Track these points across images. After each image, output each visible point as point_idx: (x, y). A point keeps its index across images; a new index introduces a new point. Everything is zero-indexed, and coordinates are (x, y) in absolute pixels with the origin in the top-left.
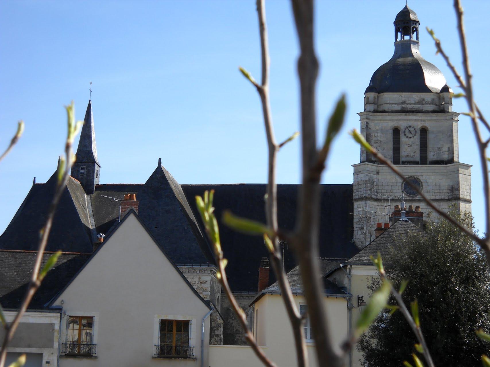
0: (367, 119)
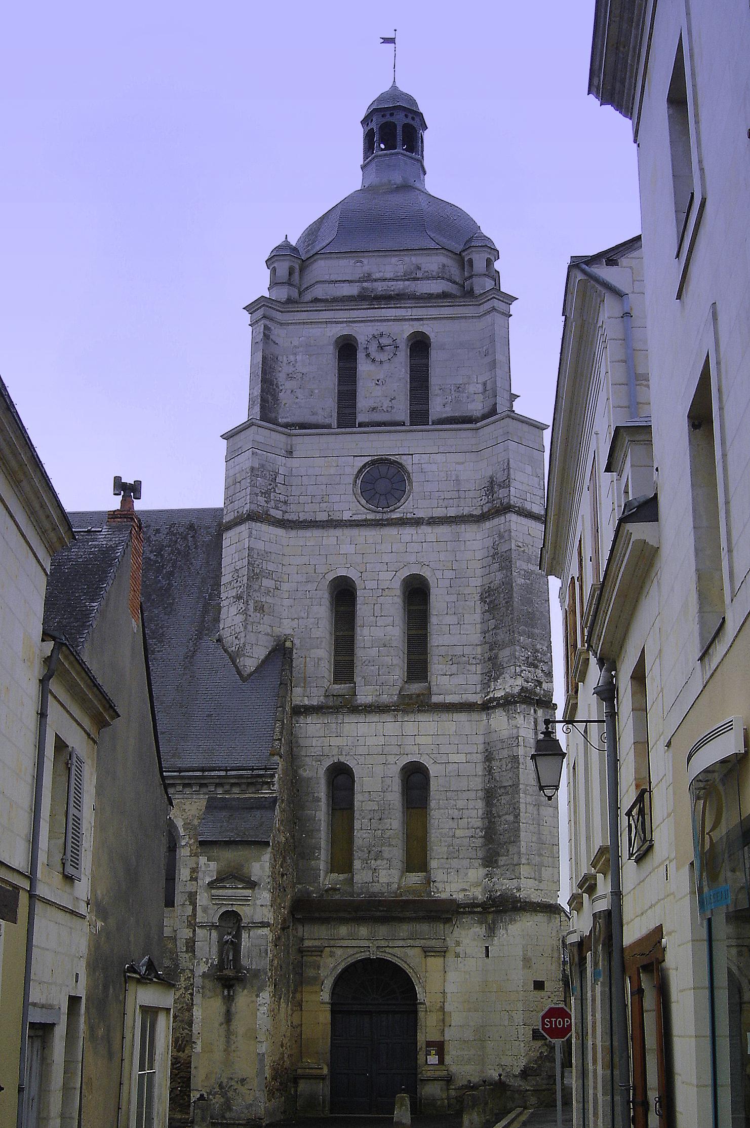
0: (264, 317)
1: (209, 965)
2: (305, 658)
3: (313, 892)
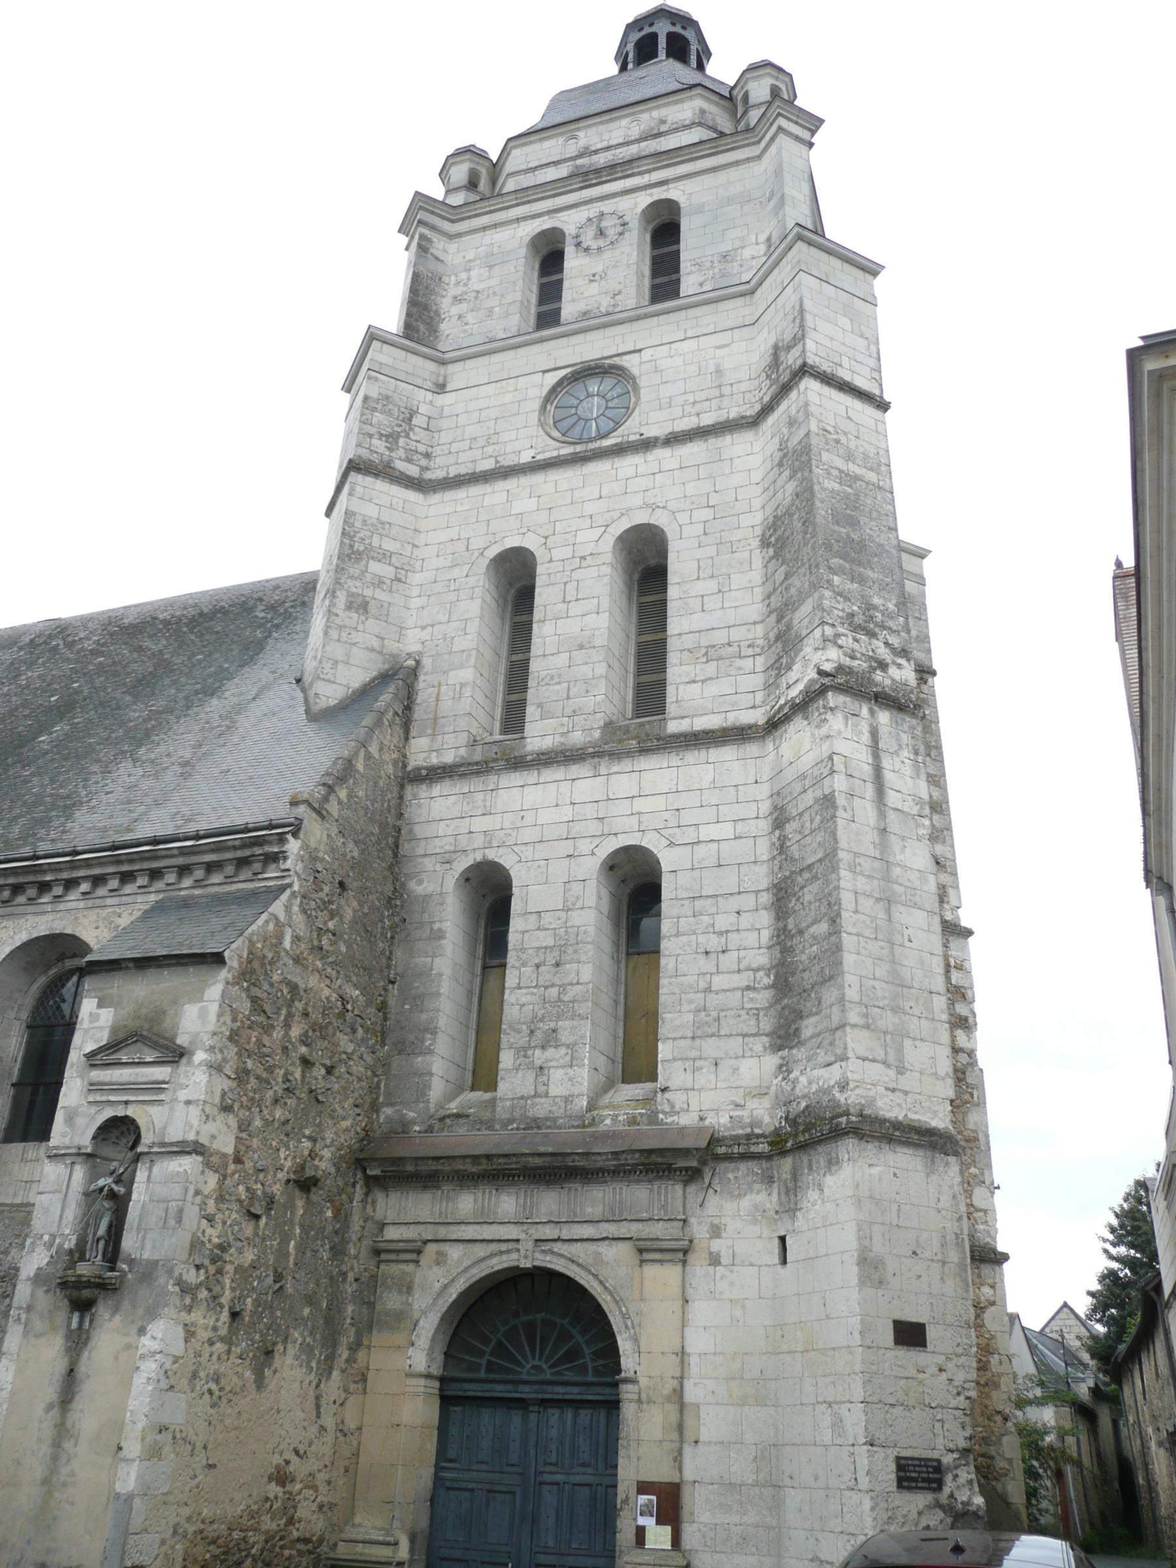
1: (54, 1250)
2: (439, 685)
3: (413, 1122)
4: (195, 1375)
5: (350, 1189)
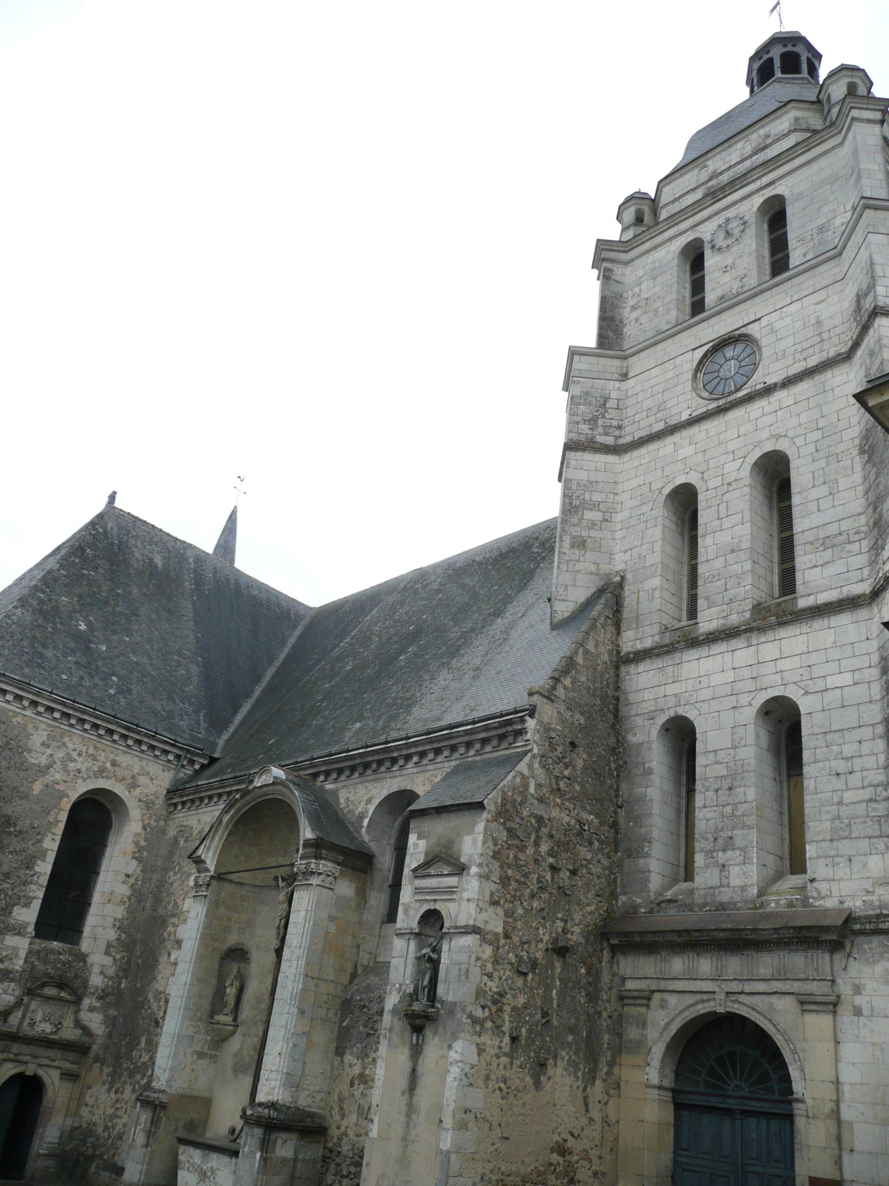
1: (401, 993)
3: (640, 906)
4: (487, 1078)
5: (599, 954)
